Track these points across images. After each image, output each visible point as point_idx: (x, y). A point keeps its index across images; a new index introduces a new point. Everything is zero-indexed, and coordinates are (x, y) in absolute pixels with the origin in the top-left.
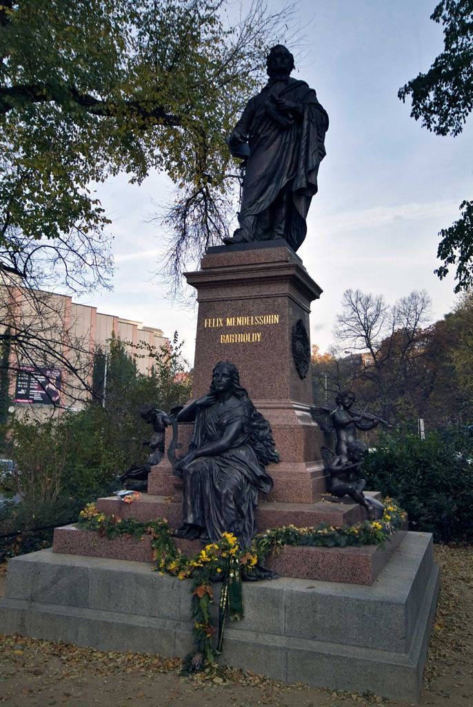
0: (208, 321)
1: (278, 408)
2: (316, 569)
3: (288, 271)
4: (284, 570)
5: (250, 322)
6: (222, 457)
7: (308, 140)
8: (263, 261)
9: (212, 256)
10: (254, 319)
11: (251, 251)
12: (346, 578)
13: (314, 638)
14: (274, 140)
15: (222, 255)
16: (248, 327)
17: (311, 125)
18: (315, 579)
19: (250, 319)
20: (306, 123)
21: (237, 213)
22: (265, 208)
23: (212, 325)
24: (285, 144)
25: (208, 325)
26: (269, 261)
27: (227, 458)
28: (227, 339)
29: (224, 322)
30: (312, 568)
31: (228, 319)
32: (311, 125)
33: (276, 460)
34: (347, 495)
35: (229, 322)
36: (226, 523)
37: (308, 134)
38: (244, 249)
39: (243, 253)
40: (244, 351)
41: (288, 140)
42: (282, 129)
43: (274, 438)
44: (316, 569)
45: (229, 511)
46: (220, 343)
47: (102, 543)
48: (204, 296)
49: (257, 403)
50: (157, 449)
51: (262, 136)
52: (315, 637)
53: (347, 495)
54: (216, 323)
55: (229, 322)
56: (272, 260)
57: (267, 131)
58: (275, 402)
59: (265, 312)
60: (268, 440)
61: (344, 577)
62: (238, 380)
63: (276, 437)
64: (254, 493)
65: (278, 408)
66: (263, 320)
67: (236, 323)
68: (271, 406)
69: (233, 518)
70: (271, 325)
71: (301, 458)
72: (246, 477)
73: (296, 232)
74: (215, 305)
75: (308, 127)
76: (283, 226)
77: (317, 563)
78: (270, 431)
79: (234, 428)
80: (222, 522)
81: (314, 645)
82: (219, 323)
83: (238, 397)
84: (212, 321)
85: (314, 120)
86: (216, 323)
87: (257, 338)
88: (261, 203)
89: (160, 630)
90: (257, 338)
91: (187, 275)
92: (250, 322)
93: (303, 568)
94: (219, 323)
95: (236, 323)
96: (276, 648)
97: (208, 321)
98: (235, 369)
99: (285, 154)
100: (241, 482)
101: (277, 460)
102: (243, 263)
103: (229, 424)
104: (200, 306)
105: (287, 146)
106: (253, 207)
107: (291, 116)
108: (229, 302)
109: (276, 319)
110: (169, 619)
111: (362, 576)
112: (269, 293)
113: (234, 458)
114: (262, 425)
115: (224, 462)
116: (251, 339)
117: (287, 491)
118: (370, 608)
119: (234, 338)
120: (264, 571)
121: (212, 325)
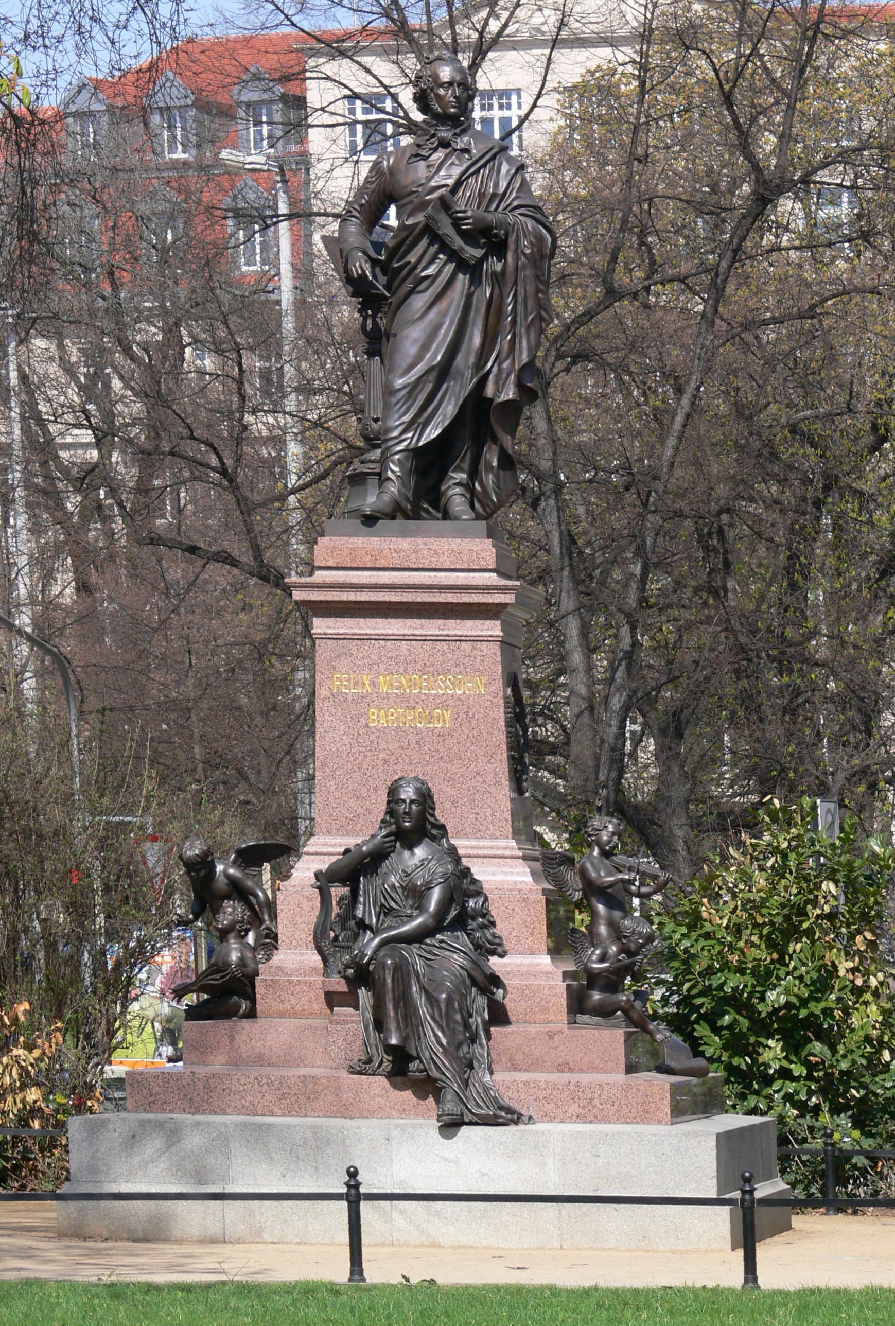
1: (494, 857)
3: (503, 596)
11: (420, 541)
16: (423, 697)
22: (433, 436)
26: (458, 566)
28: (378, 718)
33: (496, 948)
38: (404, 534)
39: (404, 544)
40: (417, 743)
49: (463, 845)
56: (466, 566)
58: (486, 845)
59: (457, 669)
60: (484, 916)
62: (434, 809)
63: (495, 911)
65: (494, 857)
69: (461, 1037)
72: (470, 975)
76: (466, 466)
79: (436, 895)
83: (434, 838)
87: (444, 721)
98: (429, 789)
100: (464, 982)
102: (405, 565)
106: (410, 435)
112: (461, 633)
113: (443, 945)
114: (472, 887)
115: (430, 953)
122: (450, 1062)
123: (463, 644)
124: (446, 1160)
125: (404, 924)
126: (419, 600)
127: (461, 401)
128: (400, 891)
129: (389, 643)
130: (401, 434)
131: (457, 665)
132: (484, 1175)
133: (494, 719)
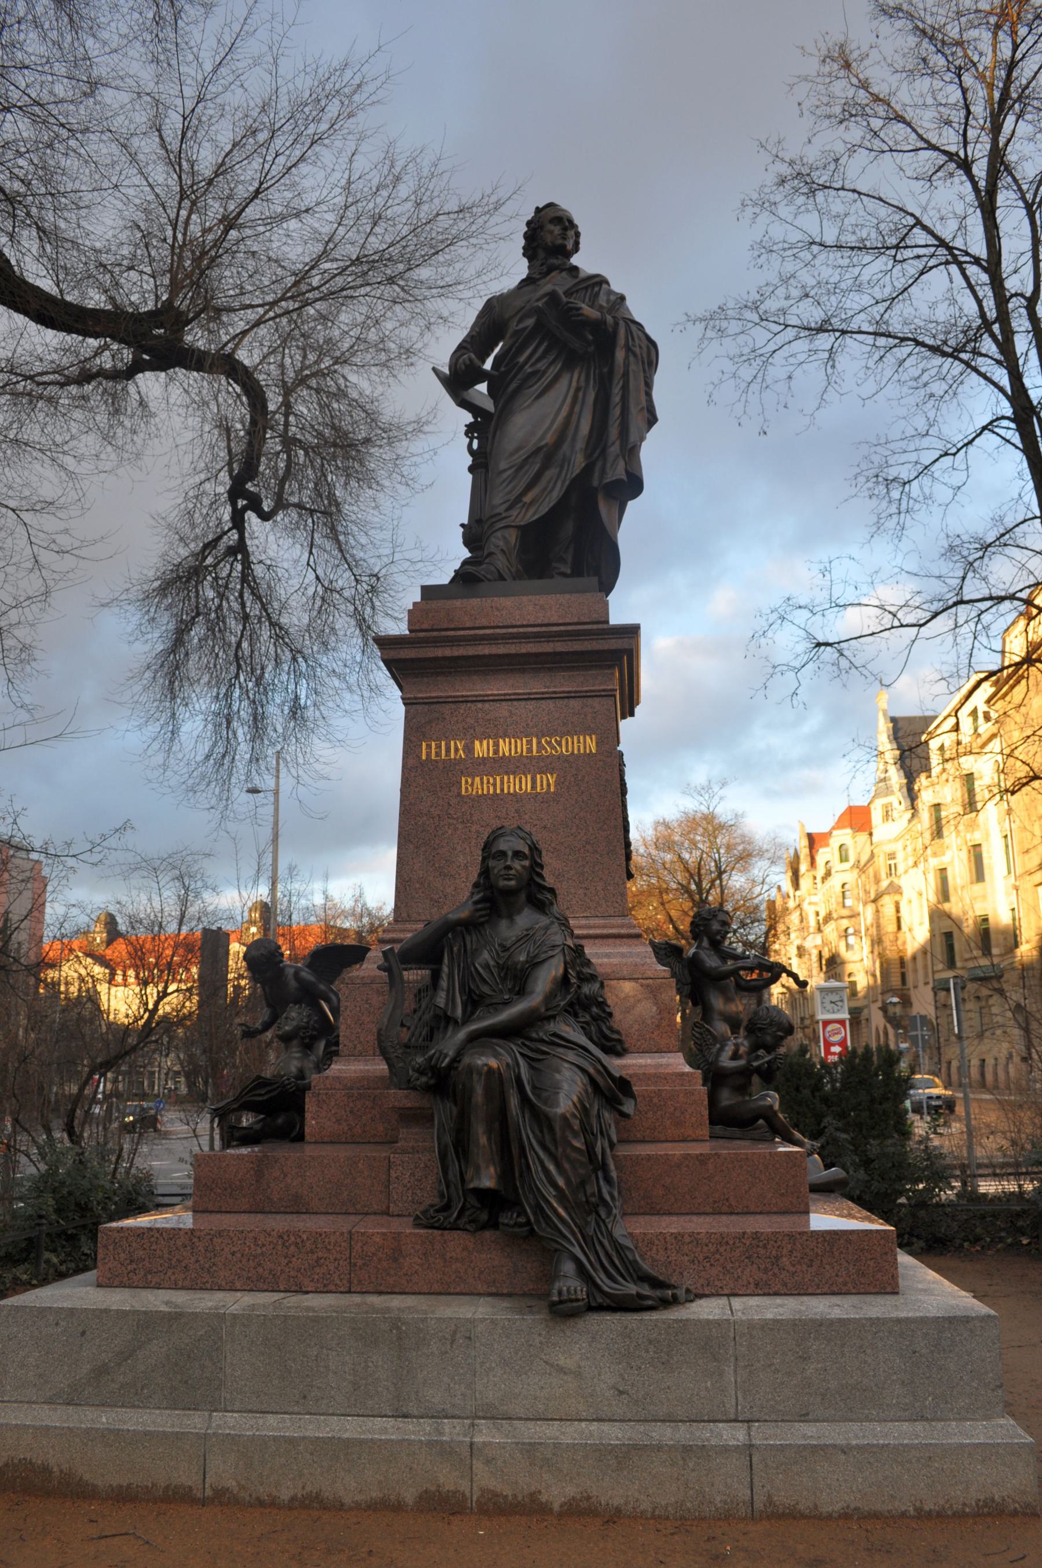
0: (429, 747)
2: (776, 1271)
4: (701, 1281)
5: (530, 750)
6: (531, 1040)
7: (625, 388)
8: (554, 619)
9: (435, 604)
10: (539, 743)
11: (525, 599)
12: (845, 1284)
13: (804, 1417)
14: (556, 379)
15: (458, 603)
16: (525, 761)
17: (632, 359)
18: (776, 1294)
19: (530, 743)
20: (620, 355)
21: (462, 525)
23: (438, 754)
24: (578, 389)
25: (429, 754)
27: (542, 1041)
28: (477, 786)
29: (469, 749)
30: (766, 1271)
31: (477, 743)
32: (632, 359)
34: (761, 1121)
35: (482, 749)
36: (568, 1182)
37: (626, 375)
41: (583, 384)
42: (571, 361)
43: (609, 1002)
44: (776, 1271)
45: (574, 1155)
46: (459, 794)
47: (233, 1254)
48: (420, 691)
50: (295, 1042)
51: (528, 369)
52: (807, 1414)
53: (761, 1121)
54: (448, 750)
55: (482, 749)
56: (576, 620)
57: (539, 360)
61: (841, 1280)
62: (542, 867)
64: (607, 1115)
66: (560, 745)
67: (496, 752)
68: (591, 932)
70: (579, 755)
71: (674, 1042)
73: (601, 566)
74: (446, 709)
75: (627, 364)
77: (777, 1258)
78: (602, 985)
80: (561, 1182)
81: (808, 1433)
82: (457, 750)
84: (439, 747)
85: (637, 350)
86: (448, 750)
87: (549, 785)
88: (531, 504)
89: (430, 1444)
90: (549, 785)
91: (385, 643)
92: (530, 750)
93: (747, 1272)
94: (457, 750)
95: (496, 752)
96: (725, 1449)
97: (429, 747)
99: (577, 409)
101: (619, 1048)
103: (535, 964)
104: (407, 712)
105: (581, 394)
106: (514, 512)
107: (590, 337)
108: (480, 705)
109: (591, 744)
110: (446, 1417)
111: (879, 1275)
116: (534, 787)
117: (650, 1114)
118: (926, 1335)
119: (494, 785)
120: (656, 1283)
121: (438, 754)
122: (566, 1209)
123: (572, 702)
124: (562, 1370)
125: (497, 1011)
126: (524, 651)
127: (567, 483)
128: (495, 971)
129: (487, 705)
130: (507, 510)
131: (564, 724)
132: (621, 1393)
133: (607, 780)
